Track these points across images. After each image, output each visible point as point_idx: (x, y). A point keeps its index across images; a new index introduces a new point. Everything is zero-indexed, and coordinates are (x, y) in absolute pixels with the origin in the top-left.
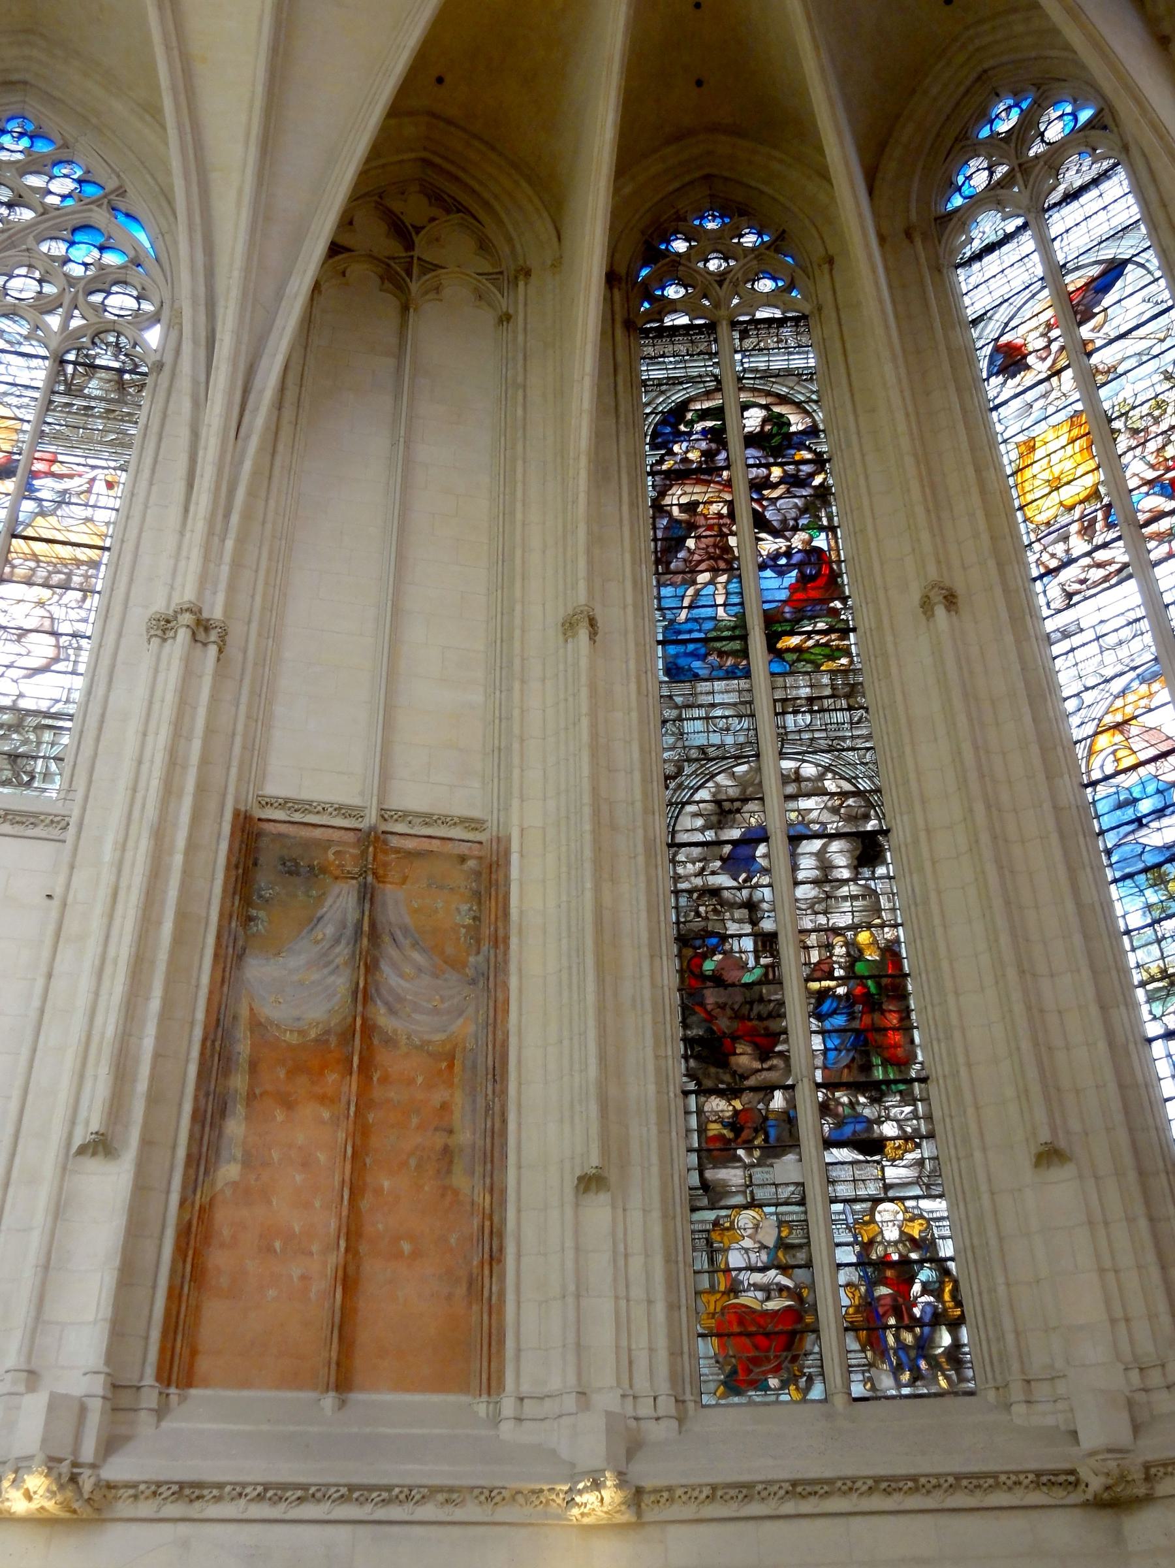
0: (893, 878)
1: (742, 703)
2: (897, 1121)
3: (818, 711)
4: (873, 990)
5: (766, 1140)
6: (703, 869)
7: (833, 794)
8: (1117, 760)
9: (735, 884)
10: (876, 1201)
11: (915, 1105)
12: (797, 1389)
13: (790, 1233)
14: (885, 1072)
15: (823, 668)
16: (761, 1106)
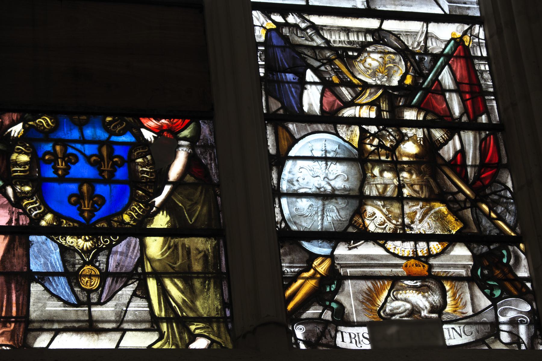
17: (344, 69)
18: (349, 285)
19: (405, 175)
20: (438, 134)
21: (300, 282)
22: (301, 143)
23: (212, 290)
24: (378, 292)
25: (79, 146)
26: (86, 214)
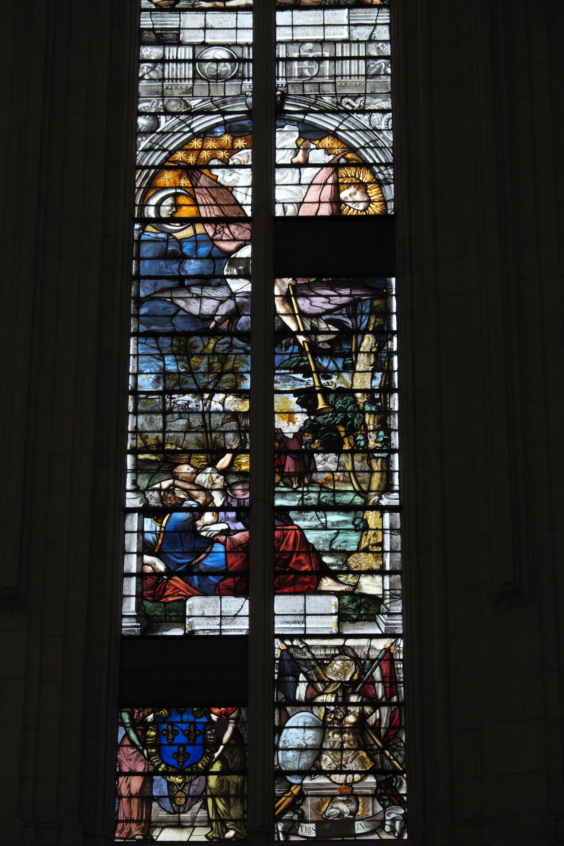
8: (176, 206)
17: (321, 672)
18: (309, 801)
19: (346, 735)
20: (367, 709)
21: (284, 798)
22: (293, 718)
23: (239, 804)
24: (323, 804)
25: (180, 725)
26: (181, 764)
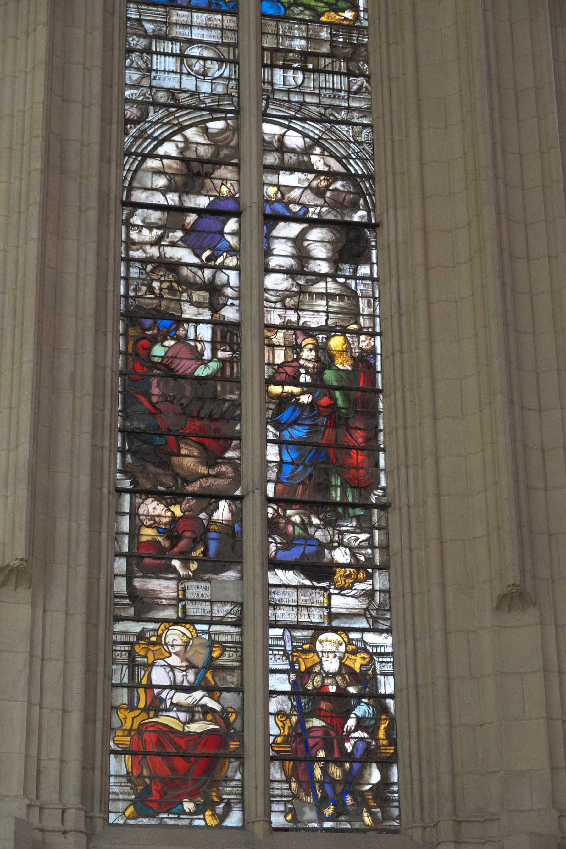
0: (377, 280)
1: (223, 44)
2: (351, 548)
3: (313, 71)
4: (340, 403)
5: (205, 553)
6: (161, 238)
7: (318, 173)
9: (196, 260)
10: (319, 629)
11: (371, 533)
12: (214, 815)
13: (222, 654)
14: (344, 494)
15: (323, 19)
16: (203, 515)
